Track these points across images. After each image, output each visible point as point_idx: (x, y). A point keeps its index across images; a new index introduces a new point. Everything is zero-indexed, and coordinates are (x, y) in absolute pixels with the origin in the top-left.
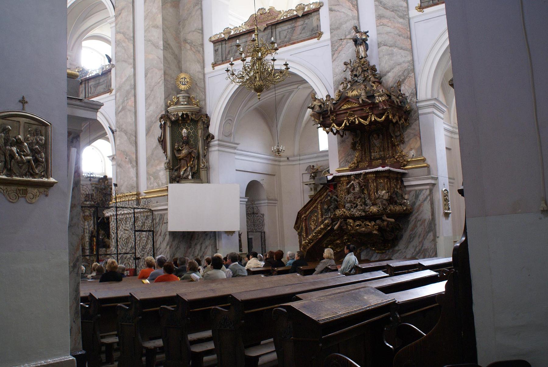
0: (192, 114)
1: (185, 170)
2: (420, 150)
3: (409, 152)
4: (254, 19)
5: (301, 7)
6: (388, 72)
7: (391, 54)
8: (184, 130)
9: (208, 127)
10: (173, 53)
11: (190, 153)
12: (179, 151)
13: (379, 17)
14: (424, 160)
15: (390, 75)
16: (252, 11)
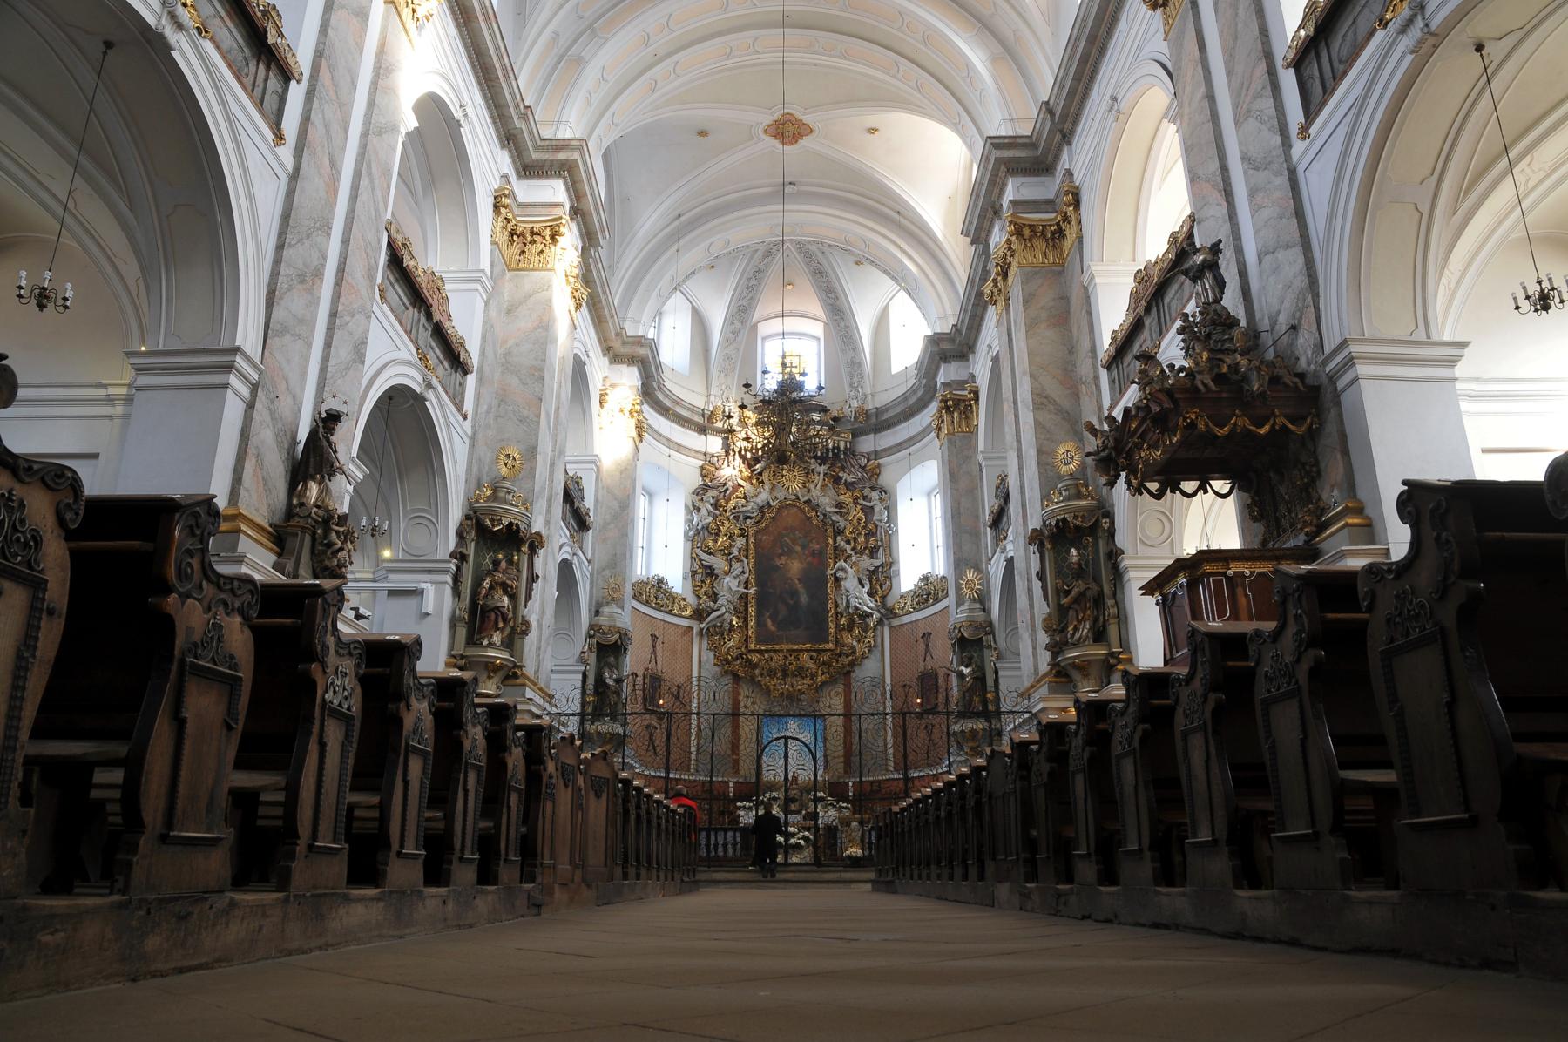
0: (1076, 517)
1: (1076, 629)
2: (1351, 487)
3: (1332, 496)
4: (1135, 296)
5: (1174, 238)
6: (1278, 312)
7: (1276, 270)
8: (1073, 551)
9: (1113, 536)
10: (1059, 410)
11: (1082, 594)
12: (1068, 593)
13: (1252, 194)
14: (1359, 511)
15: (1282, 318)
16: (1129, 283)
